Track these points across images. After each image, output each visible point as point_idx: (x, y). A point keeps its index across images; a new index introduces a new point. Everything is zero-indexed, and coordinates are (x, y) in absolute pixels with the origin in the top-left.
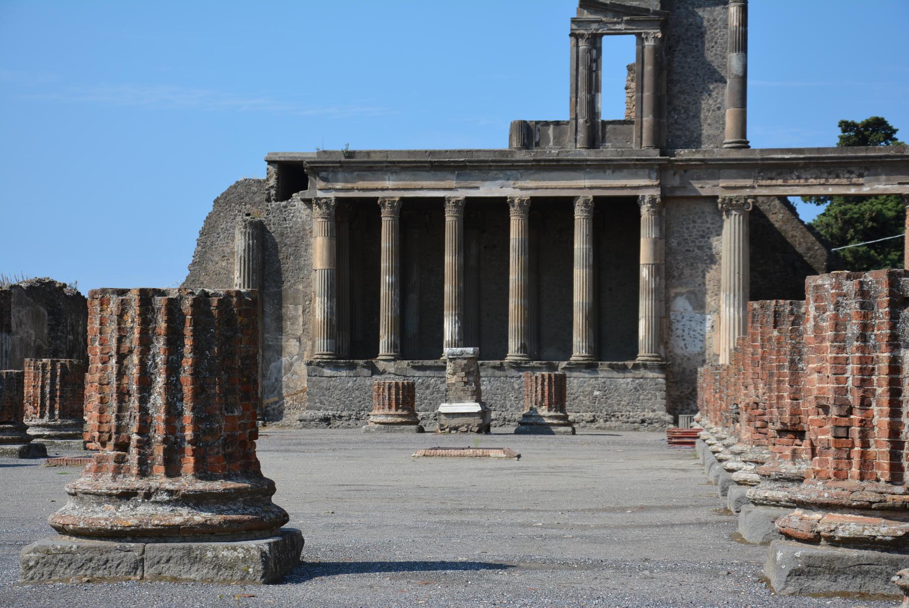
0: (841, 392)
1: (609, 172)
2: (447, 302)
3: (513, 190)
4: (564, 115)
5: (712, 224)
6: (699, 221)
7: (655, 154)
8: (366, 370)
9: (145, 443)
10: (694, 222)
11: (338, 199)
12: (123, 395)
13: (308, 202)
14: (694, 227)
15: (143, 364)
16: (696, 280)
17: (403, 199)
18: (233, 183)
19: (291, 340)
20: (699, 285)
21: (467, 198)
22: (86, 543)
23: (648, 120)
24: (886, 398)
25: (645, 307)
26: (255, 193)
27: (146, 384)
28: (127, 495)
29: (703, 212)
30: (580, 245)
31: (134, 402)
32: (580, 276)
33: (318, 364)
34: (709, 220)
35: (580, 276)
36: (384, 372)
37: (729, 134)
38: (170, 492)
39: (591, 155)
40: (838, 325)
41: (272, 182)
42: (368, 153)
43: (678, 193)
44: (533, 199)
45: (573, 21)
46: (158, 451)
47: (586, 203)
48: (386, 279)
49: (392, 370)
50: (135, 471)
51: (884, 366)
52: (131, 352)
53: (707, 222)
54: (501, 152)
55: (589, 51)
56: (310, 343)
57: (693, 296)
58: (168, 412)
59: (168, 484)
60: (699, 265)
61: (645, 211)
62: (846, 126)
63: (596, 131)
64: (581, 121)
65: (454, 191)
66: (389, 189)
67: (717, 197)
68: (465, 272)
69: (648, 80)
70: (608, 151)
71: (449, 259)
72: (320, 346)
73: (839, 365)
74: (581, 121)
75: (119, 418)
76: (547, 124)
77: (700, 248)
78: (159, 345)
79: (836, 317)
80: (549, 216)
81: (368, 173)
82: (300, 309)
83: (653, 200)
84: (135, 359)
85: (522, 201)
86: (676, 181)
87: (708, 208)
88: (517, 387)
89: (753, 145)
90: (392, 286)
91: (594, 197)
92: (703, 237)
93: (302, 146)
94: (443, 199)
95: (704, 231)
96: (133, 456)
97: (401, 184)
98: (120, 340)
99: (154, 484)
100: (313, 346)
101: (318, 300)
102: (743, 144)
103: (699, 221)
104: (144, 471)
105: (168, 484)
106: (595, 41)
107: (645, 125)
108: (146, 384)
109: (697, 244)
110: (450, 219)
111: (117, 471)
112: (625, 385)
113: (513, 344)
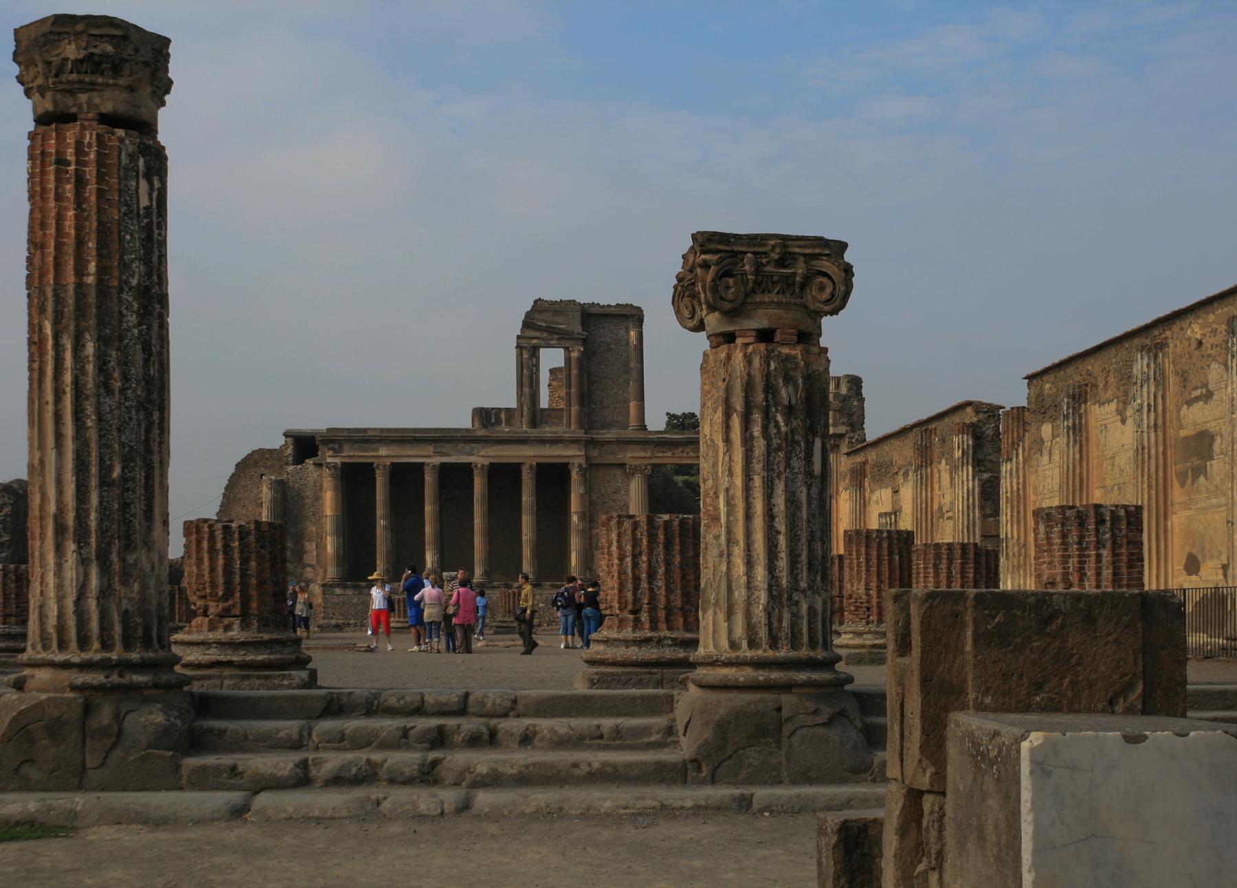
0: (1066, 575)
2: (427, 539)
4: (513, 404)
7: (581, 434)
9: (653, 609)
11: (343, 464)
12: (636, 579)
13: (319, 465)
15: (650, 561)
17: (392, 464)
21: (442, 464)
22: (630, 669)
23: (575, 409)
24: (1093, 578)
25: (575, 543)
27: (652, 575)
28: (647, 641)
30: (527, 497)
31: (644, 585)
32: (527, 521)
33: (331, 586)
35: (527, 521)
37: (633, 422)
38: (673, 639)
39: (534, 433)
40: (1064, 536)
41: (290, 451)
42: (366, 430)
43: (597, 461)
44: (491, 464)
45: (518, 337)
46: (662, 614)
47: (531, 466)
48: (381, 523)
50: (647, 626)
51: (1093, 559)
52: (641, 553)
54: (467, 430)
55: (531, 359)
56: (321, 570)
58: (666, 590)
59: (668, 634)
61: (575, 474)
62: (671, 417)
63: (537, 417)
64: (525, 409)
65: (431, 458)
66: (385, 454)
68: (441, 517)
69: (574, 381)
70: (548, 431)
71: (428, 508)
72: (332, 572)
73: (1065, 559)
74: (525, 409)
75: (635, 594)
76: (500, 410)
78: (660, 549)
79: (1062, 531)
80: (504, 478)
83: (580, 466)
84: (644, 558)
85: (483, 466)
86: (595, 453)
87: (618, 472)
89: (650, 428)
90: (385, 528)
91: (538, 464)
93: (315, 422)
94: (423, 464)
96: (644, 617)
97: (391, 453)
98: (634, 546)
99: (662, 634)
100: (325, 571)
101: (329, 538)
102: (643, 427)
104: (654, 628)
105: (668, 634)
106: (534, 352)
107: (573, 412)
108: (652, 575)
110: (429, 479)
111: (635, 627)
113: (478, 571)
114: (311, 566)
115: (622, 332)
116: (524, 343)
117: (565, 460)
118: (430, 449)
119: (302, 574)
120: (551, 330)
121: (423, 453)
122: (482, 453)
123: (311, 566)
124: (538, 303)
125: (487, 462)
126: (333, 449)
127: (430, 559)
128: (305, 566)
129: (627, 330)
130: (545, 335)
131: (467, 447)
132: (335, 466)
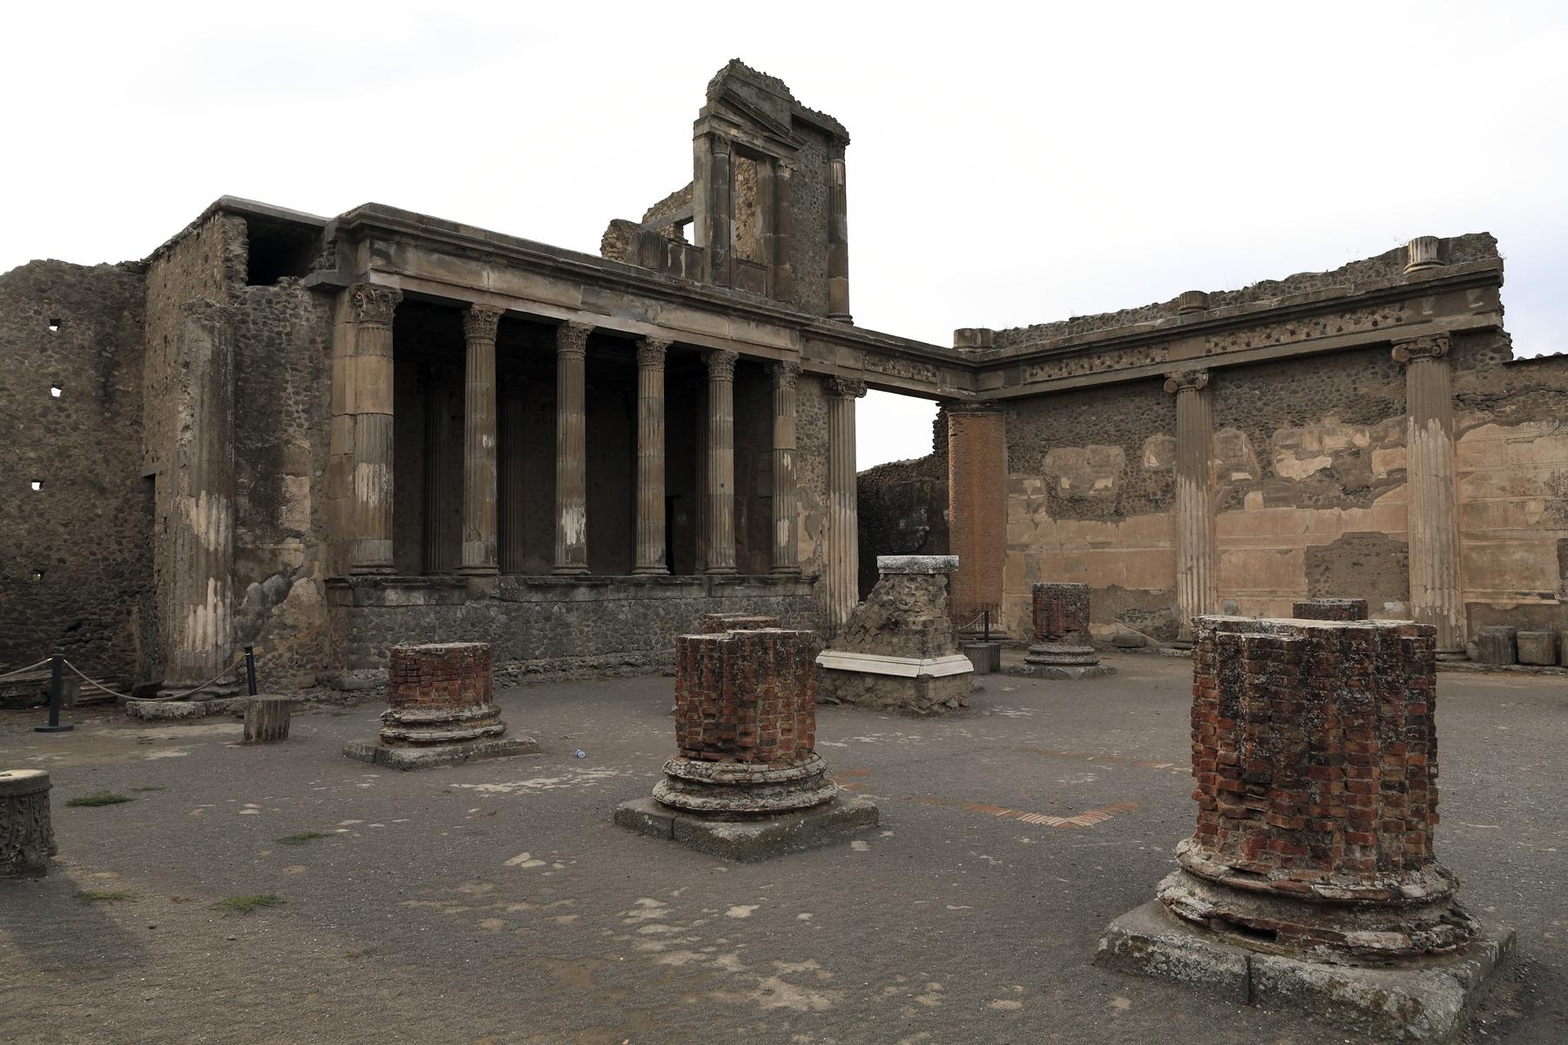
1: (753, 324)
3: (661, 325)
8: (457, 593)
18: (24, 262)
19: (290, 540)
26: (71, 286)
36: (483, 596)
42: (456, 226)
49: (496, 592)
61: (785, 383)
67: (832, 376)
77: (808, 436)
81: (455, 260)
82: (306, 482)
83: (795, 369)
87: (814, 389)
88: (662, 612)
90: (489, 451)
101: (364, 470)
102: (848, 320)
114: (298, 535)
115: (818, 162)
116: (722, 130)
117: (775, 356)
118: (575, 295)
119: (274, 553)
120: (758, 121)
121: (563, 299)
122: (659, 320)
123: (298, 535)
124: (732, 62)
125: (669, 337)
126: (384, 255)
127: (572, 525)
128: (282, 535)
129: (828, 160)
130: (748, 126)
131: (639, 304)
132: (384, 295)
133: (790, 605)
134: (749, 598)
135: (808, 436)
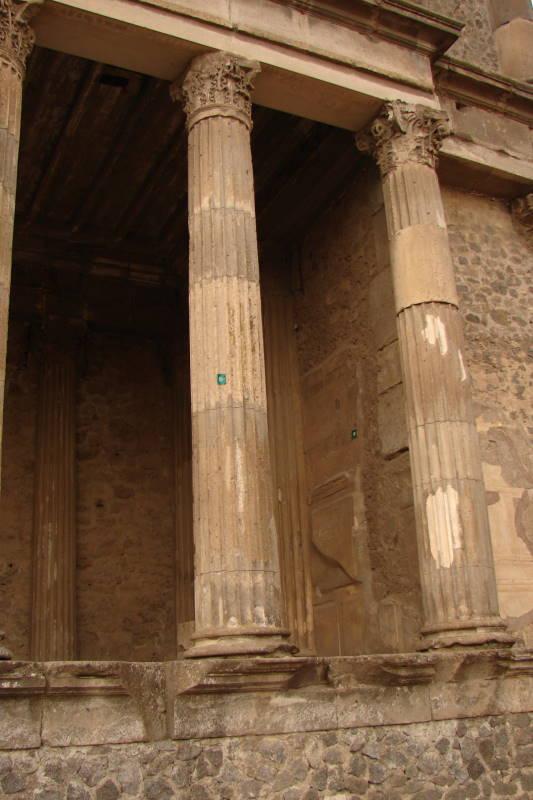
5: (517, 261)
6: (485, 248)
10: (474, 247)
14: (477, 261)
16: (504, 400)
20: (513, 415)
29: (490, 229)
34: (507, 250)
53: (505, 256)
57: (504, 447)
60: (505, 361)
77: (498, 317)
92: (501, 289)
95: (500, 276)
103: (485, 248)
109: (491, 306)
112: (432, 754)
133: (485, 747)
134: (329, 735)
135: (498, 317)
